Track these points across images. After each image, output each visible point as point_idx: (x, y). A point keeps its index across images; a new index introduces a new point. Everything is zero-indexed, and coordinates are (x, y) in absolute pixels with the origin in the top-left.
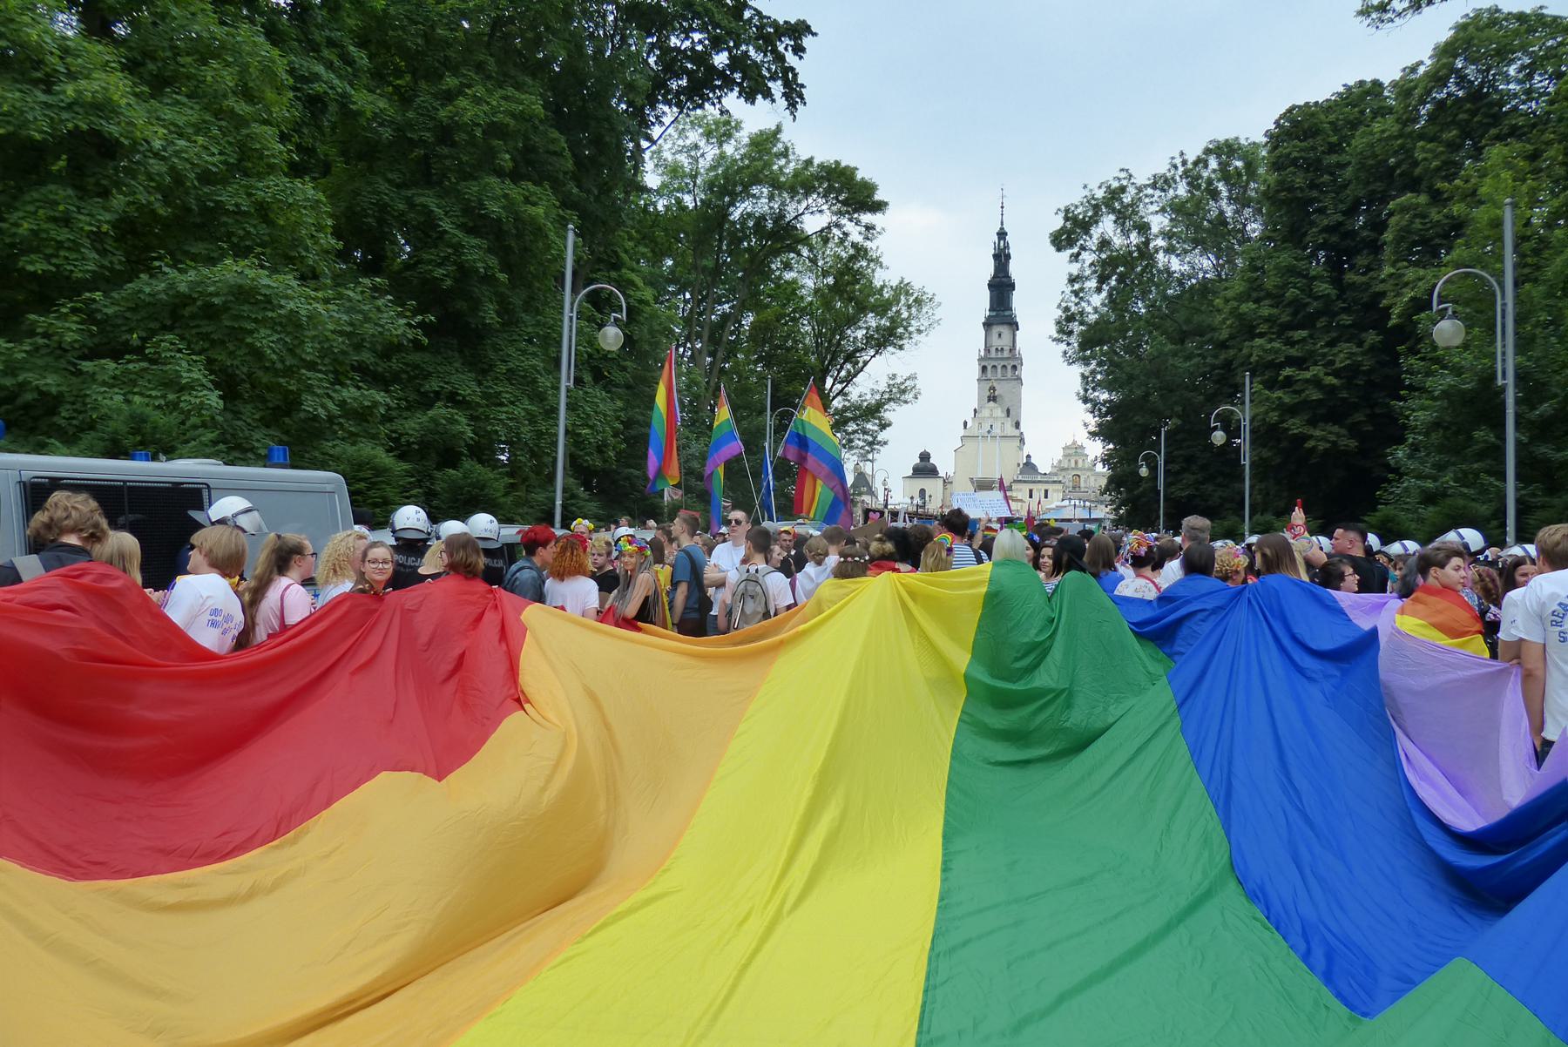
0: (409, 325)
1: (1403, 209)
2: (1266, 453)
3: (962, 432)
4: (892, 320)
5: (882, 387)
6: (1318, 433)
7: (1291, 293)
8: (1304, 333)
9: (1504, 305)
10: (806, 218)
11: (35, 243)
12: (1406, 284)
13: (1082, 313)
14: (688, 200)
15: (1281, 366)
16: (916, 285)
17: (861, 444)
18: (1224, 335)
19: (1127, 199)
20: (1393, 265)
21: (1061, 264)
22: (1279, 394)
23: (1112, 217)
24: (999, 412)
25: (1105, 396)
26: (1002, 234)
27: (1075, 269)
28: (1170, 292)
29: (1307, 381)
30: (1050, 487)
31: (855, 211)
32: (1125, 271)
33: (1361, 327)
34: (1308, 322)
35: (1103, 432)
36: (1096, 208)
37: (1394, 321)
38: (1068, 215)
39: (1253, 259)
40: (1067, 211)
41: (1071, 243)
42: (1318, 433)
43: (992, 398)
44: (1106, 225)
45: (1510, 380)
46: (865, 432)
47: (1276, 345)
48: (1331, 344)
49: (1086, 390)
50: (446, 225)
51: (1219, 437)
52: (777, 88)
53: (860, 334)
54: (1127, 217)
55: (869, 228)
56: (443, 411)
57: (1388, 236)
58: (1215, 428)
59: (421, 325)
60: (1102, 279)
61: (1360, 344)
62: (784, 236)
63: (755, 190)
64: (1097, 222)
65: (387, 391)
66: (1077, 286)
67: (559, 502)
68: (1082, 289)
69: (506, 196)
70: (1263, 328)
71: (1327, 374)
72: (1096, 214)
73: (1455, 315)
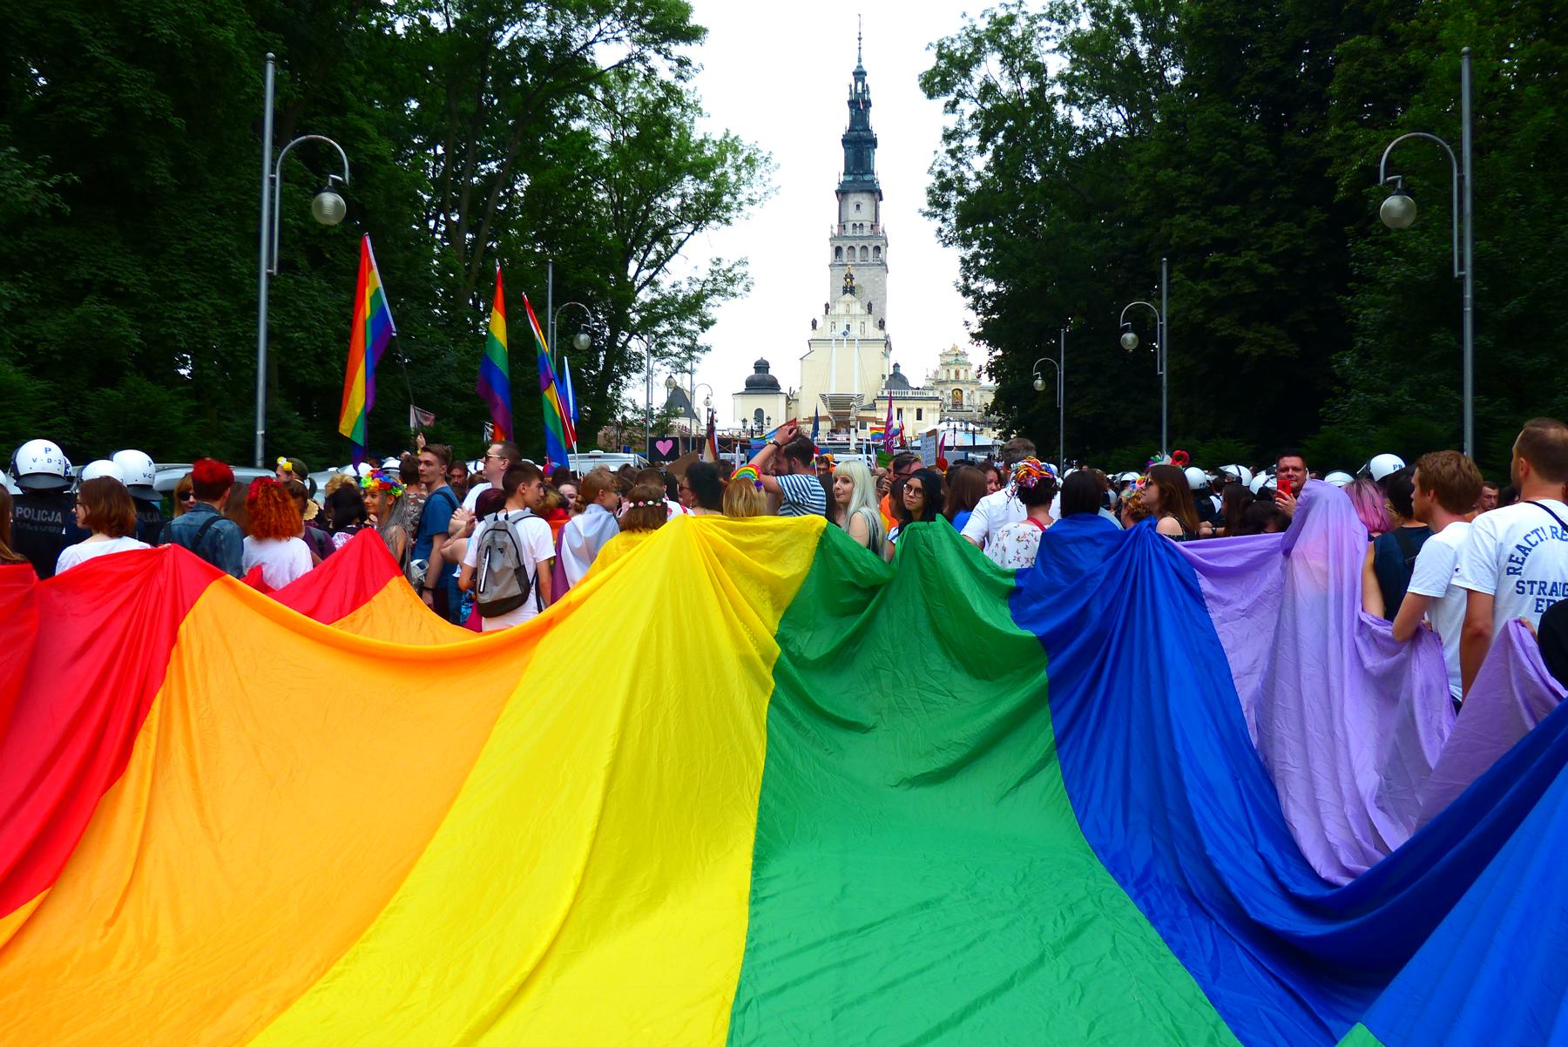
0: (43, 188)
1: (1353, 55)
3: (811, 334)
4: (716, 184)
5: (703, 274)
6: (1251, 335)
7: (1219, 157)
8: (1234, 209)
9: (1461, 178)
10: (598, 48)
12: (1355, 150)
13: (961, 179)
14: (438, 21)
15: (1208, 249)
16: (746, 141)
17: (675, 349)
18: (1138, 209)
19: (1016, 32)
20: (1340, 125)
21: (934, 116)
22: (1204, 285)
23: (998, 56)
24: (858, 308)
25: (990, 287)
26: (860, 75)
27: (951, 122)
28: (1072, 153)
29: (1238, 269)
30: (923, 405)
31: (665, 39)
32: (1016, 125)
35: (988, 334)
36: (978, 43)
37: (1341, 195)
39: (1173, 114)
40: (941, 46)
41: (946, 87)
42: (1251, 335)
43: (849, 289)
44: (991, 67)
45: (1468, 272)
47: (1201, 223)
48: (1267, 223)
49: (966, 279)
50: (96, 50)
53: (673, 203)
54: (1017, 55)
55: (682, 63)
56: (96, 308)
57: (1334, 88)
58: (1126, 330)
59: (60, 187)
60: (986, 136)
61: (1301, 225)
62: (568, 71)
63: (529, 8)
64: (978, 61)
65: (14, 280)
66: (954, 144)
67: (260, 432)
68: (960, 148)
69: (180, 12)
70: (1185, 201)
71: (1262, 261)
72: (977, 50)
73: (1407, 191)
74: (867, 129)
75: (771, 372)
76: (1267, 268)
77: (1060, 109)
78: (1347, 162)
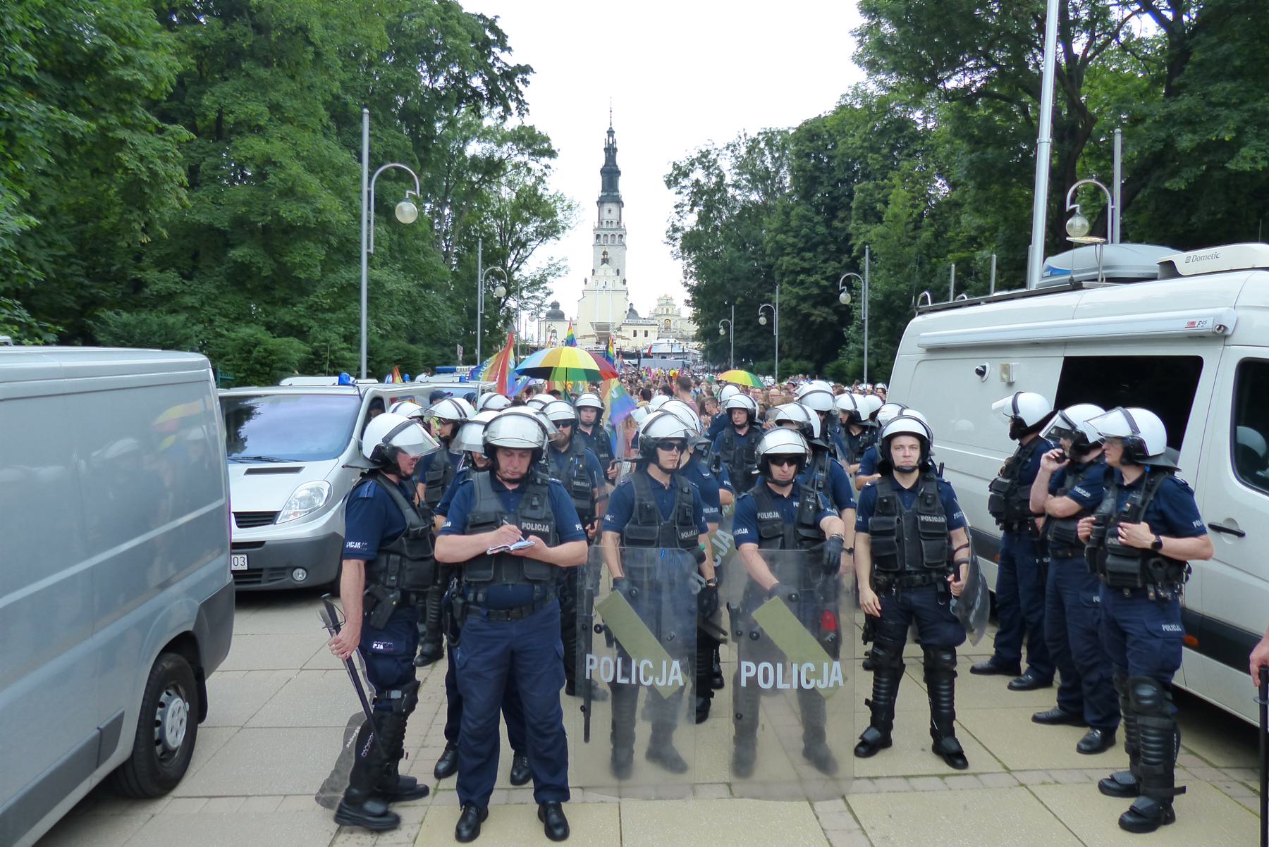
1: (862, 191)
2: (790, 323)
3: (583, 287)
5: (545, 266)
7: (804, 231)
11: (301, 265)
15: (798, 273)
16: (568, 196)
19: (712, 157)
21: (672, 197)
24: (611, 273)
26: (611, 133)
27: (679, 199)
32: (709, 198)
33: (839, 251)
34: (813, 248)
35: (694, 303)
38: (676, 167)
41: (676, 182)
43: (605, 261)
44: (698, 174)
46: (537, 298)
47: (796, 260)
48: (825, 261)
51: (763, 321)
52: (513, 105)
55: (547, 167)
60: (694, 204)
70: (789, 250)
74: (615, 165)
75: (561, 308)
76: (824, 283)
77: (731, 191)
78: (858, 238)
